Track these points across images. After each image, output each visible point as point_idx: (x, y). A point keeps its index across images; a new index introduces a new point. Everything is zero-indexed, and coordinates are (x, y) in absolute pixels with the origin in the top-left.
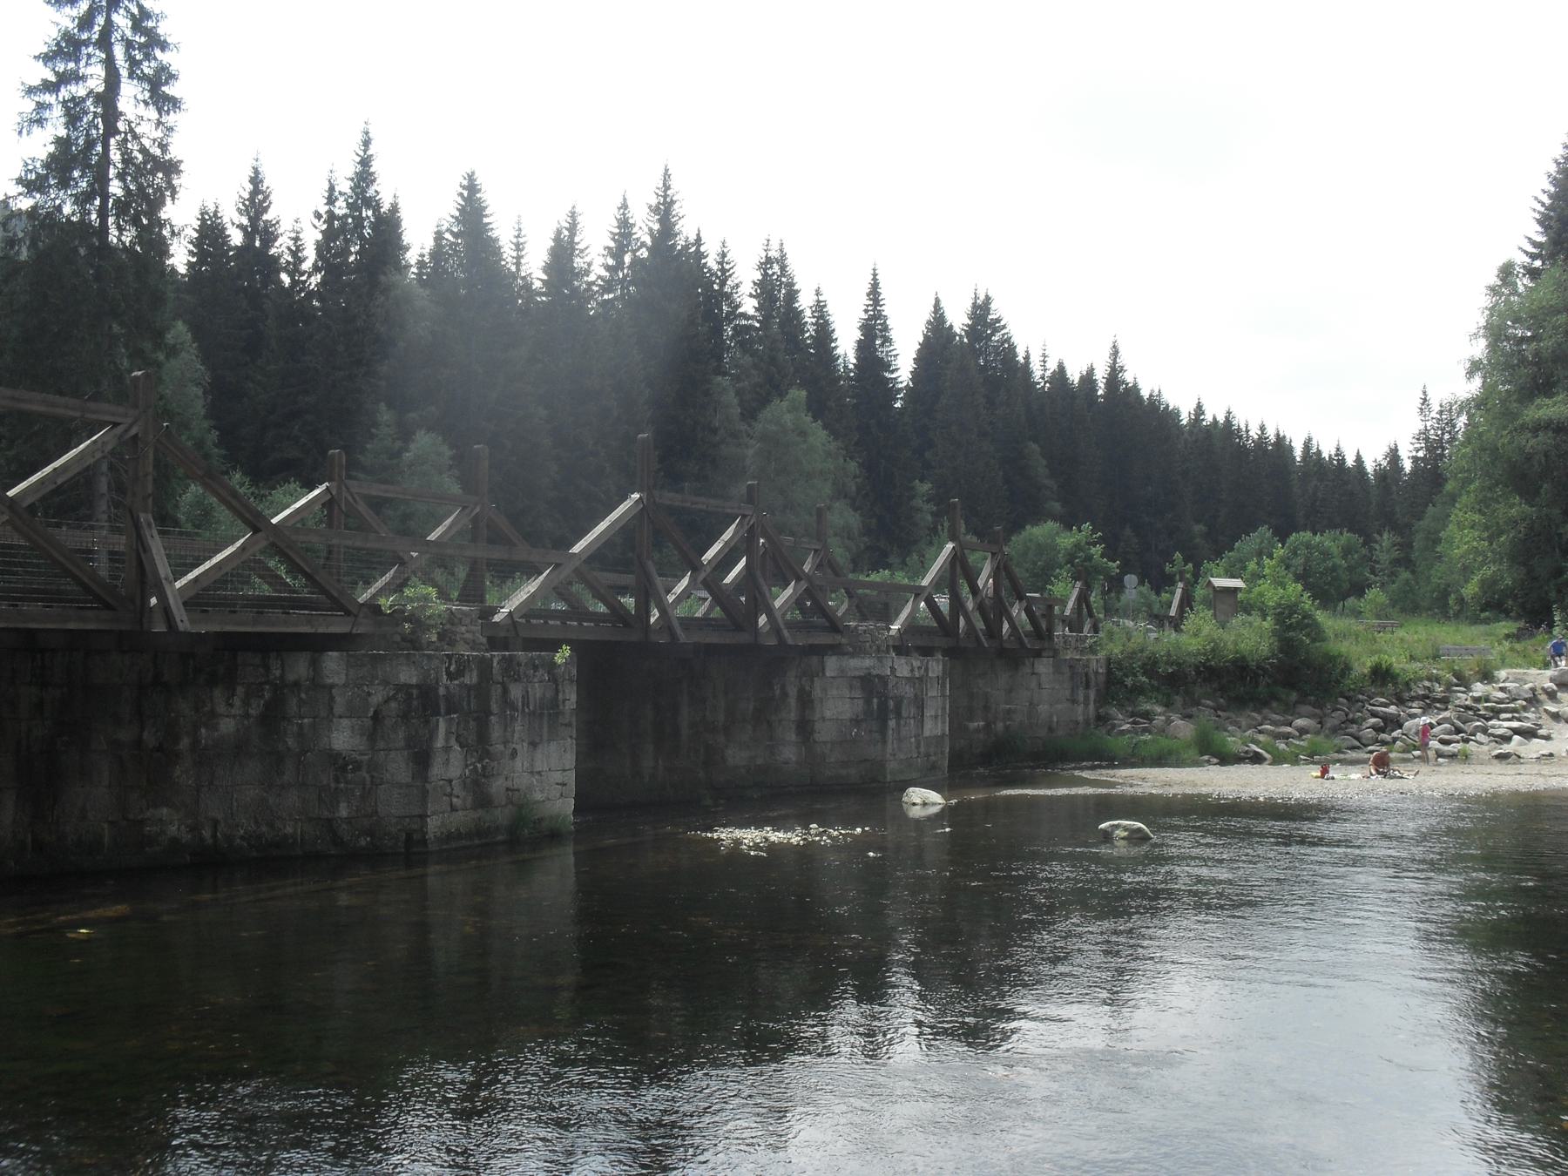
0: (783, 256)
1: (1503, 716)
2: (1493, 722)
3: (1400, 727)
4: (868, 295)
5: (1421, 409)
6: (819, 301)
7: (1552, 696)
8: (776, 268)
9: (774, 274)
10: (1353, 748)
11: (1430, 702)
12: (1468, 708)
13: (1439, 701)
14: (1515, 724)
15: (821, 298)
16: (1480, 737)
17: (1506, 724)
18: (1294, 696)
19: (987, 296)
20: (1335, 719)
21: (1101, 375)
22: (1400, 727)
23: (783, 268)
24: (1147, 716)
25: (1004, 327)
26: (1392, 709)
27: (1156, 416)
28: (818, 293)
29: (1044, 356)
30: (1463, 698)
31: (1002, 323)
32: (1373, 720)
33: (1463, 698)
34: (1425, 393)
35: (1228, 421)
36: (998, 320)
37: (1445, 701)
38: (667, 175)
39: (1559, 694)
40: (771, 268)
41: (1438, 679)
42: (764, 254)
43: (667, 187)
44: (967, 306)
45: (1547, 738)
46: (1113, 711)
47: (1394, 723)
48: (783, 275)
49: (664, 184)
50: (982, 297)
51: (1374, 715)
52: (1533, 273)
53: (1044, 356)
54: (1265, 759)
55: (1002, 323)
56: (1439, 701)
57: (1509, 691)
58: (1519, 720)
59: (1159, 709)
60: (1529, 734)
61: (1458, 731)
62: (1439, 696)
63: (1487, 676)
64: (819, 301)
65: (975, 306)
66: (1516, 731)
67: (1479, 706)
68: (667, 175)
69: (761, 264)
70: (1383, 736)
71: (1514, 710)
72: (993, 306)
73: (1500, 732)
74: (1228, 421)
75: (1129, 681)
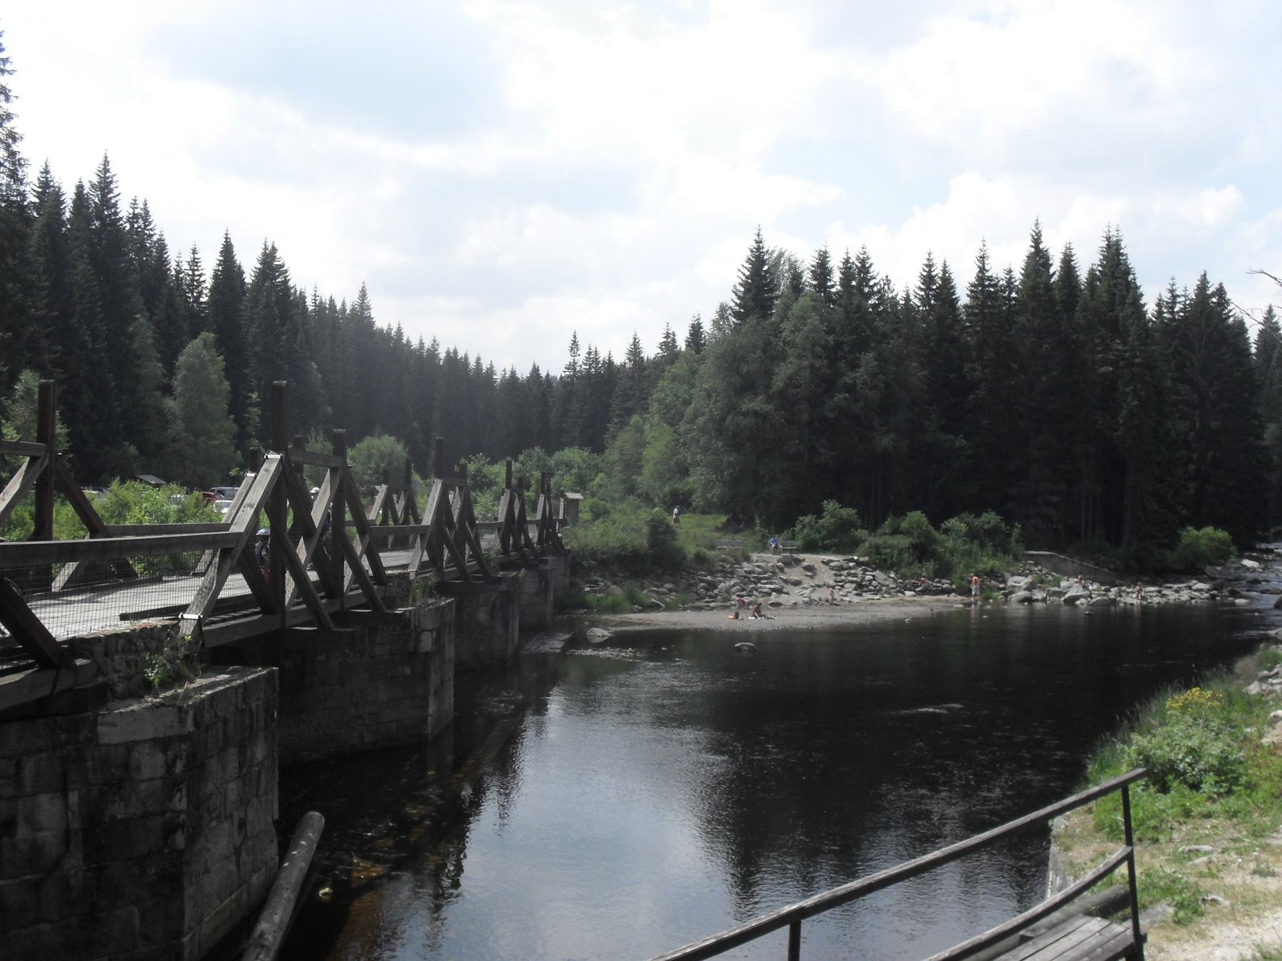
0: (147, 212)
1: (763, 581)
2: (759, 585)
3: (716, 588)
4: (221, 252)
6: (194, 259)
7: (782, 570)
8: (141, 222)
9: (139, 227)
10: (697, 600)
11: (729, 574)
12: (745, 577)
13: (728, 573)
14: (772, 586)
15: (196, 256)
16: (755, 592)
17: (768, 586)
18: (660, 571)
20: (683, 583)
21: (395, 329)
22: (716, 588)
23: (145, 220)
24: (596, 582)
25: (286, 271)
26: (709, 578)
27: (484, 378)
28: (194, 252)
29: (315, 295)
30: (741, 572)
31: (284, 268)
32: (702, 584)
33: (741, 572)
35: (513, 373)
36: (282, 266)
37: (732, 573)
38: (106, 162)
39: (786, 570)
40: (137, 222)
41: (724, 560)
42: (131, 211)
43: (106, 170)
44: (258, 253)
45: (788, 593)
46: (578, 580)
47: (712, 586)
48: (146, 226)
49: (104, 169)
50: (270, 248)
51: (702, 581)
52: (736, 315)
53: (315, 295)
54: (661, 607)
55: (284, 268)
56: (728, 573)
57: (763, 568)
58: (771, 584)
59: (600, 579)
60: (779, 591)
61: (743, 590)
62: (729, 570)
63: (748, 559)
64: (194, 259)
65: (265, 254)
66: (773, 590)
67: (750, 576)
68: (106, 162)
69: (130, 218)
70: (710, 593)
71: (767, 578)
72: (278, 255)
73: (765, 590)
74: (513, 373)
75: (585, 563)
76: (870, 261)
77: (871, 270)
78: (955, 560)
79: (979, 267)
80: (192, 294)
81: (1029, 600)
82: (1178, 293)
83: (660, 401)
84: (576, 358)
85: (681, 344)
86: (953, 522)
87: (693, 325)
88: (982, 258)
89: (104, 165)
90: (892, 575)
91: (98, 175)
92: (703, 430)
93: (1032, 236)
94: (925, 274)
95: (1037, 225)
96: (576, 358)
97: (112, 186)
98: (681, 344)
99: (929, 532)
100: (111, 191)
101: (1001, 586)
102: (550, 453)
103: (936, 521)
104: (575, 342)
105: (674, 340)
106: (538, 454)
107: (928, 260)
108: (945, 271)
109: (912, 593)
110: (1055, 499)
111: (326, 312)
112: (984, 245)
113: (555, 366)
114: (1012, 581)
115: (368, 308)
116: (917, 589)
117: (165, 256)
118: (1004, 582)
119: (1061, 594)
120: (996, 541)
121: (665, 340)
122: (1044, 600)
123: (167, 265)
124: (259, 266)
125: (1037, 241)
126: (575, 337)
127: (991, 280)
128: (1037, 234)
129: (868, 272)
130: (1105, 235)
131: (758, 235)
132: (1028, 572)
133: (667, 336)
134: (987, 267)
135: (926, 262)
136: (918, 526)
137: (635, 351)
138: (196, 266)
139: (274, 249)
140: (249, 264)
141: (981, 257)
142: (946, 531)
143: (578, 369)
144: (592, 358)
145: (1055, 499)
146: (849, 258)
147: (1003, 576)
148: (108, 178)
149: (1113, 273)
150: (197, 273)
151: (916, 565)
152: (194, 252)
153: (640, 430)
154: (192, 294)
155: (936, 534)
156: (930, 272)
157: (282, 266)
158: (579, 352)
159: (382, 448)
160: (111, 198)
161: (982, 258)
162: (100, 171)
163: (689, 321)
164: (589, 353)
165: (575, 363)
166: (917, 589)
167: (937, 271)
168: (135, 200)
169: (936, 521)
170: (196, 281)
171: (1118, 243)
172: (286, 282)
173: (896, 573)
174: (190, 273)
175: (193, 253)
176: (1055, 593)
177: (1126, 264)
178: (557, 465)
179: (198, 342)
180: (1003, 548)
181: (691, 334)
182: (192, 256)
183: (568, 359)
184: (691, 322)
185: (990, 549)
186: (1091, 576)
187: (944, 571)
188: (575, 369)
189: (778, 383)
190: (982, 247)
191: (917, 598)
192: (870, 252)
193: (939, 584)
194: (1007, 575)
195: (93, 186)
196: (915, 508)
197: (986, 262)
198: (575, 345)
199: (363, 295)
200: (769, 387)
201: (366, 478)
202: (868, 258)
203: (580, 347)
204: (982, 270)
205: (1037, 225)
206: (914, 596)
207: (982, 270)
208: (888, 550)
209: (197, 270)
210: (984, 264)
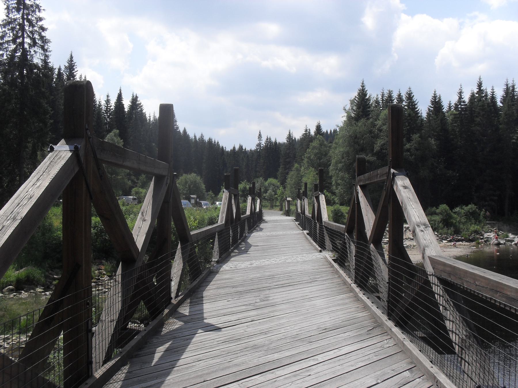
5: (259, 137)
6: (108, 99)
15: (109, 98)
25: (142, 106)
29: (154, 116)
31: (141, 105)
34: (260, 133)
36: (140, 104)
38: (72, 57)
44: (130, 98)
50: (135, 96)
53: (154, 116)
55: (141, 105)
64: (108, 99)
68: (72, 57)
72: (138, 99)
77: (413, 98)
78: (461, 226)
79: (459, 97)
80: (107, 114)
81: (498, 244)
83: (309, 158)
84: (261, 141)
85: (312, 133)
86: (457, 209)
87: (317, 126)
89: (71, 58)
90: (436, 233)
91: (68, 63)
92: (340, 170)
93: (478, 84)
94: (433, 100)
95: (480, 79)
96: (261, 141)
97: (74, 67)
98: (312, 133)
99: (450, 213)
100: (74, 69)
101: (482, 237)
102: (266, 180)
103: (452, 208)
104: (260, 135)
105: (310, 133)
106: (261, 181)
107: (434, 94)
109: (446, 241)
110: (496, 198)
112: (461, 87)
113: (251, 145)
114: (486, 235)
116: (448, 240)
117: (94, 99)
118: (482, 235)
119: (512, 241)
120: (473, 216)
121: (305, 132)
122: (505, 244)
123: (95, 103)
124: (130, 104)
126: (260, 133)
127: (465, 103)
128: (480, 83)
129: (412, 99)
130: (505, 83)
131: (363, 83)
132: (490, 230)
133: (306, 131)
134: (463, 97)
135: (433, 95)
136: (445, 211)
137: (290, 137)
138: (109, 102)
139: (137, 97)
140: (127, 103)
141: (460, 92)
142: (455, 213)
143: (262, 146)
144: (268, 140)
145: (496, 198)
146: (400, 94)
147: (481, 233)
148: (73, 64)
150: (109, 105)
151: (445, 230)
152: (108, 96)
153: (298, 170)
154: (107, 114)
155: (452, 214)
157: (140, 104)
158: (262, 139)
159: (192, 179)
160: (74, 73)
162: (69, 61)
163: (316, 124)
164: (267, 139)
165: (260, 143)
166: (448, 240)
168: (81, 76)
169: (452, 208)
170: (109, 109)
172: (142, 110)
173: (438, 232)
174: (106, 105)
175: (107, 97)
176: (509, 241)
178: (269, 185)
179: (112, 134)
180: (478, 221)
181: (316, 130)
182: (107, 98)
183: (257, 142)
184: (317, 125)
185: (473, 221)
186: (515, 232)
187: (457, 232)
188: (260, 146)
189: (377, 148)
190: (460, 88)
191: (448, 244)
192: (413, 90)
193: (457, 237)
194: (483, 232)
195: (66, 67)
196: (443, 203)
197: (462, 95)
198: (260, 136)
200: (373, 150)
201: (185, 192)
202: (412, 93)
205: (480, 79)
206: (447, 243)
207: (460, 98)
208: (433, 222)
209: (109, 104)
210: (461, 96)
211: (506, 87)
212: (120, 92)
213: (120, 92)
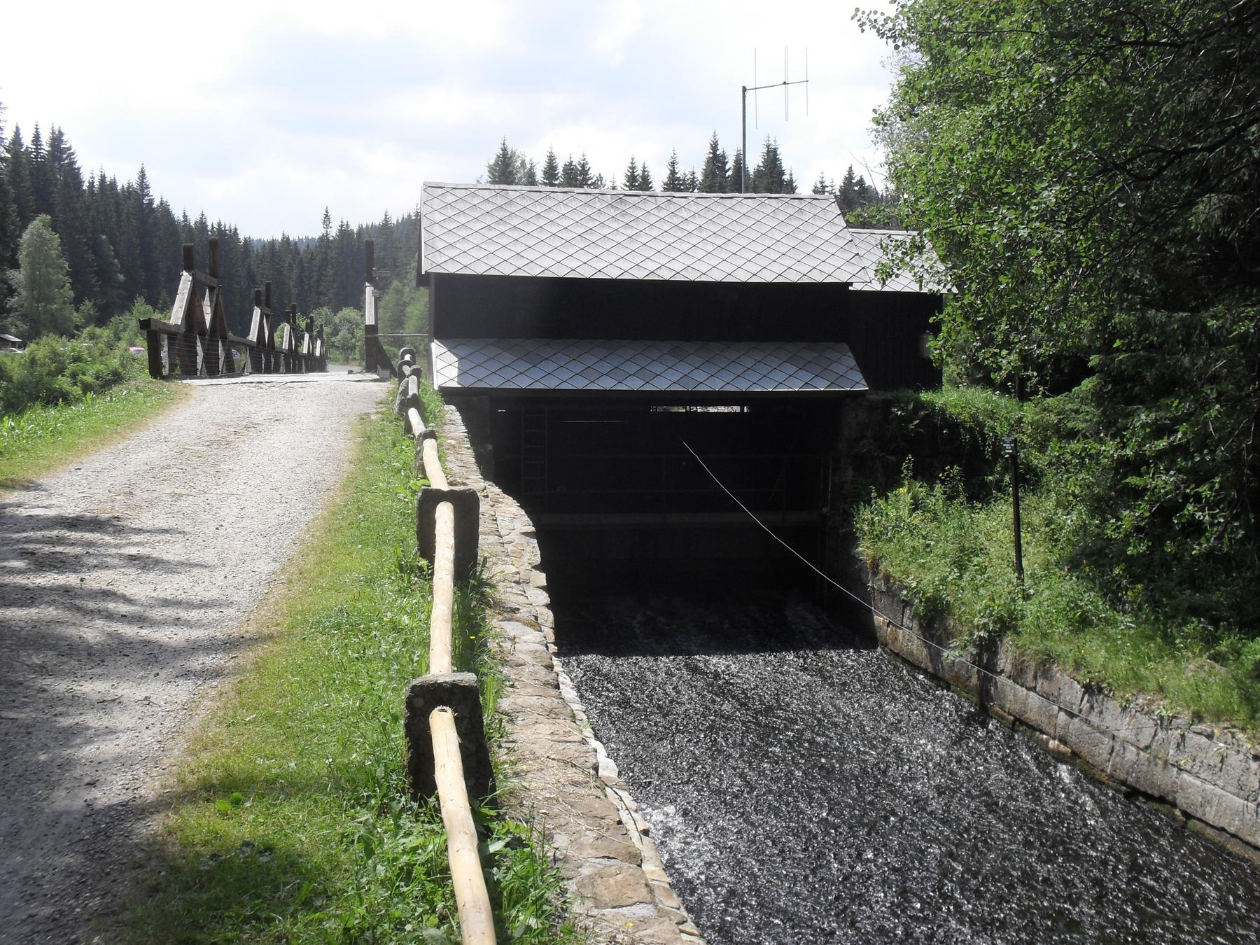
19: (60, 131)
25: (73, 154)
36: (69, 149)
72: (64, 138)
76: (588, 166)
82: (825, 184)
88: (673, 164)
102: (336, 312)
108: (644, 172)
111: (107, 188)
115: (148, 187)
125: (714, 147)
139: (61, 134)
149: (771, 173)
153: (399, 292)
156: (633, 172)
161: (673, 164)
164: (342, 226)
167: (639, 172)
171: (775, 150)
172: (72, 163)
177: (781, 167)
178: (340, 321)
192: (589, 159)
199: (143, 175)
203: (332, 220)
204: (673, 172)
205: (714, 136)
207: (673, 172)
211: (765, 150)
212: (37, 132)
213: (37, 132)
